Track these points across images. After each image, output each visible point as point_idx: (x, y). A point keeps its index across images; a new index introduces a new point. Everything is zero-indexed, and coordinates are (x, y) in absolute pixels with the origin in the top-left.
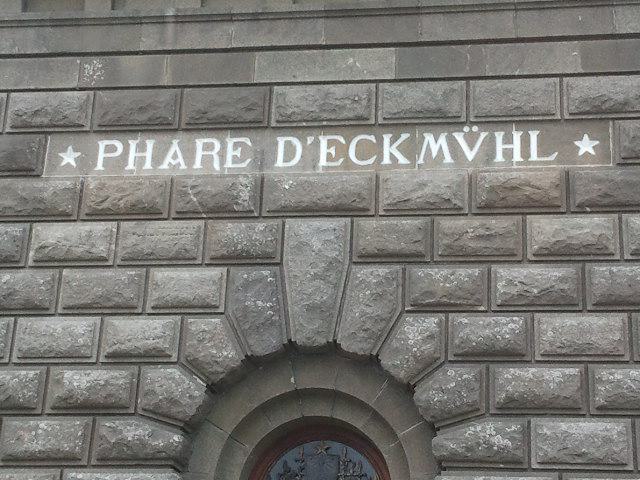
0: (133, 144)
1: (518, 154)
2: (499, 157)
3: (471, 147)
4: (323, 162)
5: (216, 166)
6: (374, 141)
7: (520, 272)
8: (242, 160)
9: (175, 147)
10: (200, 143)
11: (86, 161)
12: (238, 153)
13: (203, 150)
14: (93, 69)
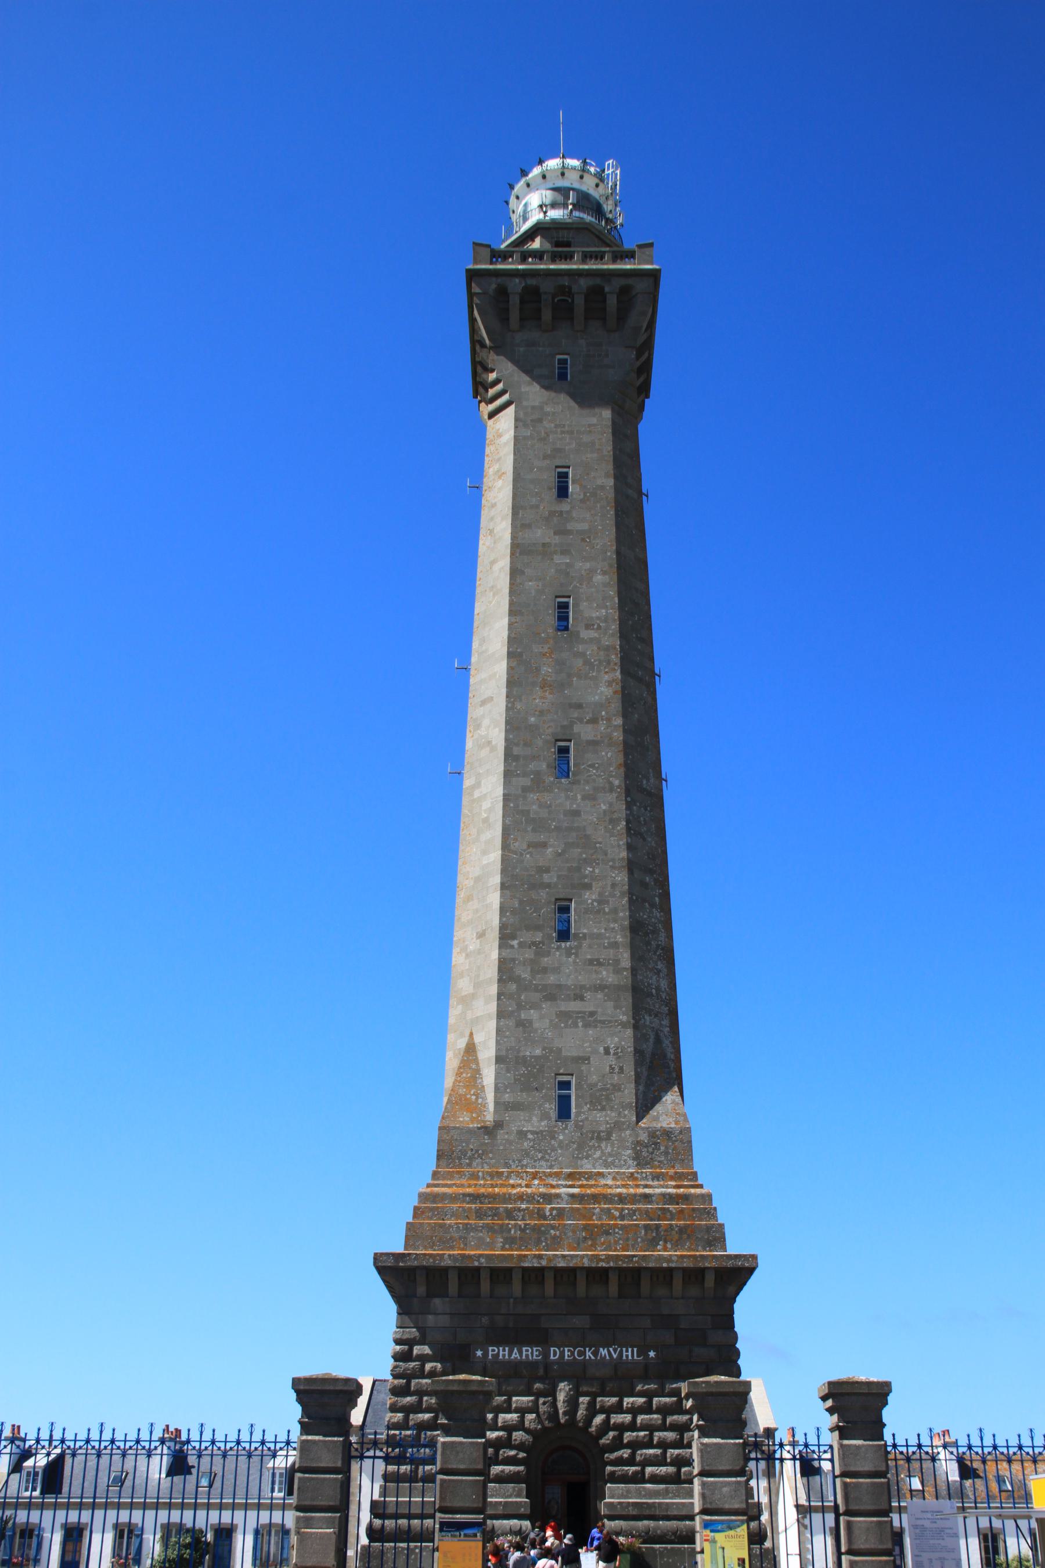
1: (630, 1354)
7: (631, 1399)
10: (524, 1349)
11: (486, 1354)
14: (485, 1320)
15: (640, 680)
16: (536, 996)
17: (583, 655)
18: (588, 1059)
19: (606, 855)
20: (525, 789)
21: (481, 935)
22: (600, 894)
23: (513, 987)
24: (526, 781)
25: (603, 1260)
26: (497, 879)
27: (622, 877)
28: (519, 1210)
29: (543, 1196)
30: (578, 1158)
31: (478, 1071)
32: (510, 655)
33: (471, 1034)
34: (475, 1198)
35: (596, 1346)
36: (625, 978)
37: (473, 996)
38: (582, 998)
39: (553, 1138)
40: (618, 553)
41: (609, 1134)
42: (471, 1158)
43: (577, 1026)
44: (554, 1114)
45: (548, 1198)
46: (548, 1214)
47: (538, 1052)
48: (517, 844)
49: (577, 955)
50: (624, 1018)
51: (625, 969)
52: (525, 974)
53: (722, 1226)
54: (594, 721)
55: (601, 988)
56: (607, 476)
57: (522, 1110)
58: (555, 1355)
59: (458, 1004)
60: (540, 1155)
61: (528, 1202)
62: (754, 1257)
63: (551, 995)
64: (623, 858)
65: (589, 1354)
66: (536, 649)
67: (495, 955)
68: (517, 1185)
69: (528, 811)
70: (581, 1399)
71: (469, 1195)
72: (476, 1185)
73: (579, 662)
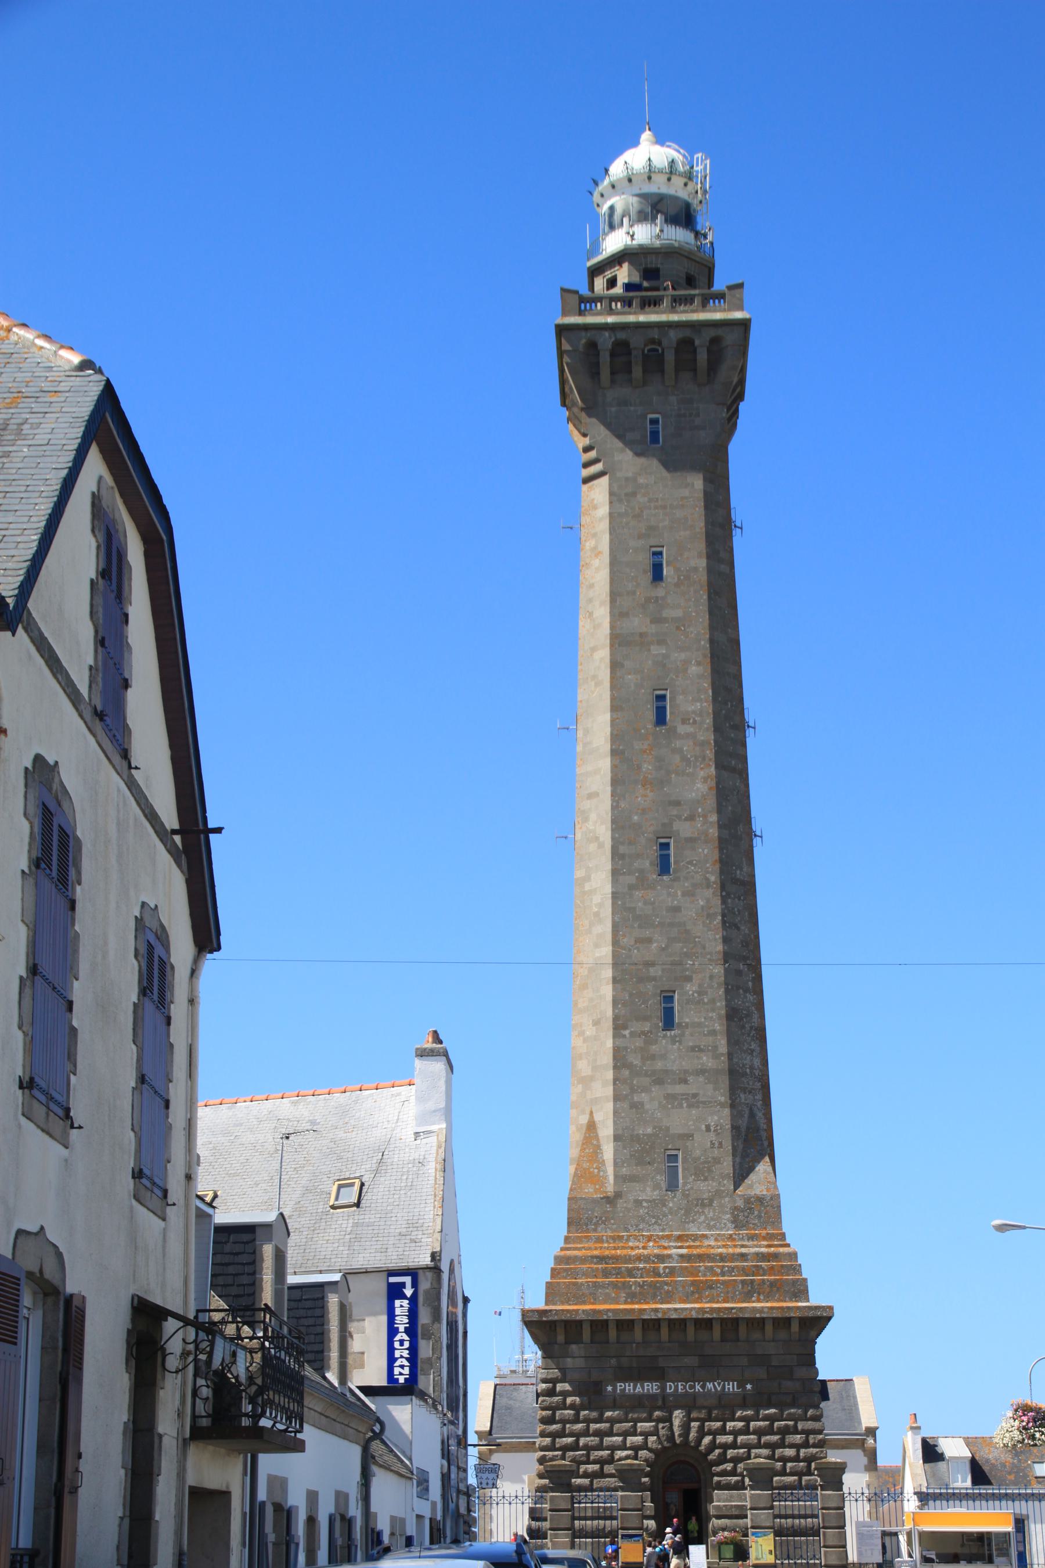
1: (731, 1387)
7: (733, 1424)
14: (613, 1361)
15: (733, 770)
16: (646, 1081)
17: (680, 751)
18: (692, 1136)
19: (704, 948)
20: (631, 887)
21: (596, 1023)
22: (700, 986)
23: (626, 1073)
24: (631, 880)
26: (608, 973)
27: (719, 970)
28: (638, 1269)
29: (658, 1256)
30: (685, 1222)
31: (598, 1147)
32: (614, 753)
33: (591, 1113)
34: (601, 1259)
35: (703, 1381)
36: (723, 1063)
37: (592, 1078)
38: (685, 1081)
39: (664, 1205)
40: (712, 641)
41: (711, 1201)
42: (596, 1224)
43: (681, 1106)
44: (664, 1186)
45: (662, 1258)
47: (649, 1130)
48: (625, 940)
49: (680, 1042)
50: (723, 1099)
51: (722, 1055)
52: (635, 1060)
53: (805, 1280)
54: (691, 818)
55: (702, 1072)
56: (700, 556)
57: (638, 1182)
59: (579, 1083)
60: (653, 1221)
61: (645, 1262)
62: (831, 1308)
63: (659, 1081)
64: (719, 952)
65: (698, 1387)
66: (638, 745)
67: (610, 1043)
68: (636, 1248)
69: (634, 908)
70: (693, 1424)
71: (597, 1257)
72: (601, 1248)
73: (677, 758)
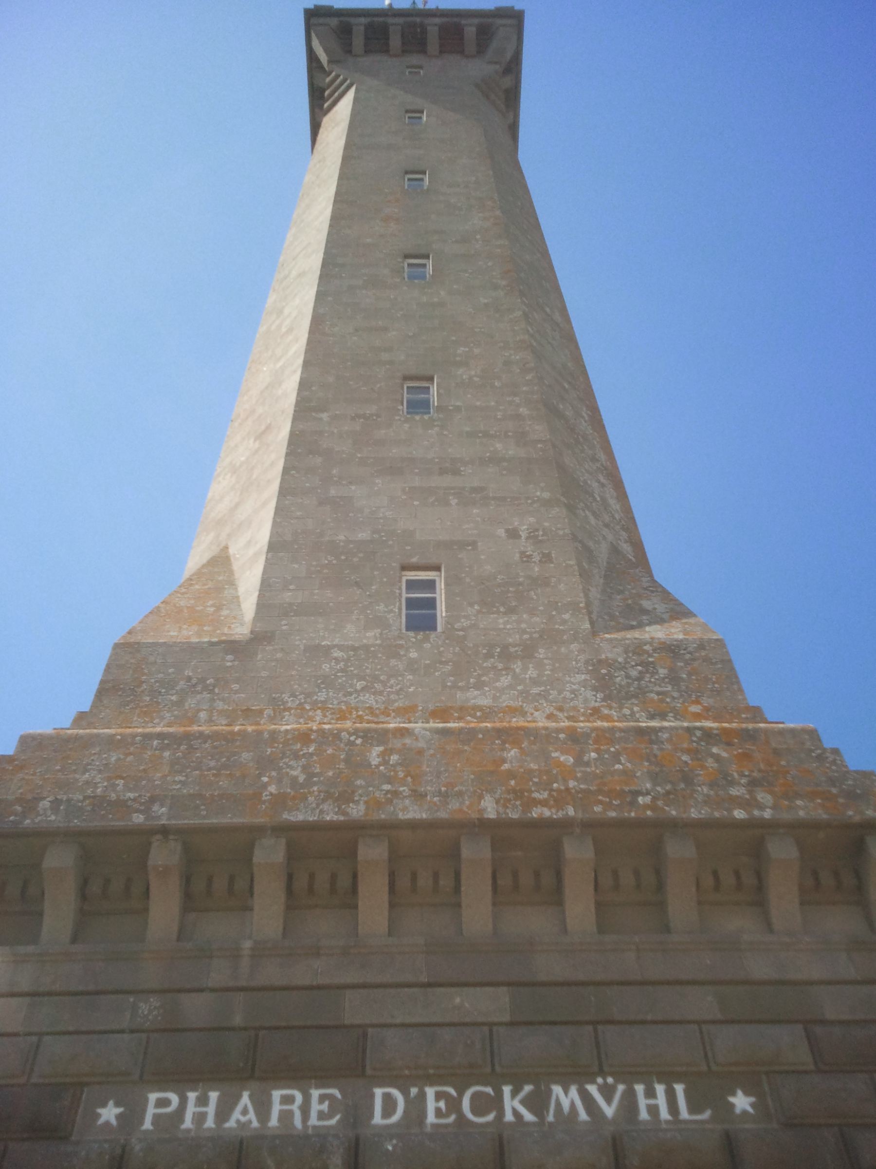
0: (192, 1096)
2: (644, 1115)
3: (609, 1101)
4: (431, 1118)
5: (298, 1122)
6: (492, 1093)
8: (330, 1116)
9: (245, 1099)
11: (132, 1116)
12: (325, 1107)
13: (281, 1103)
18: (474, 544)
25: (544, 803)
30: (455, 686)
35: (537, 1076)
38: (456, 472)
43: (447, 504)
46: (375, 761)
50: (546, 495)
58: (388, 1111)
63: (393, 470)
